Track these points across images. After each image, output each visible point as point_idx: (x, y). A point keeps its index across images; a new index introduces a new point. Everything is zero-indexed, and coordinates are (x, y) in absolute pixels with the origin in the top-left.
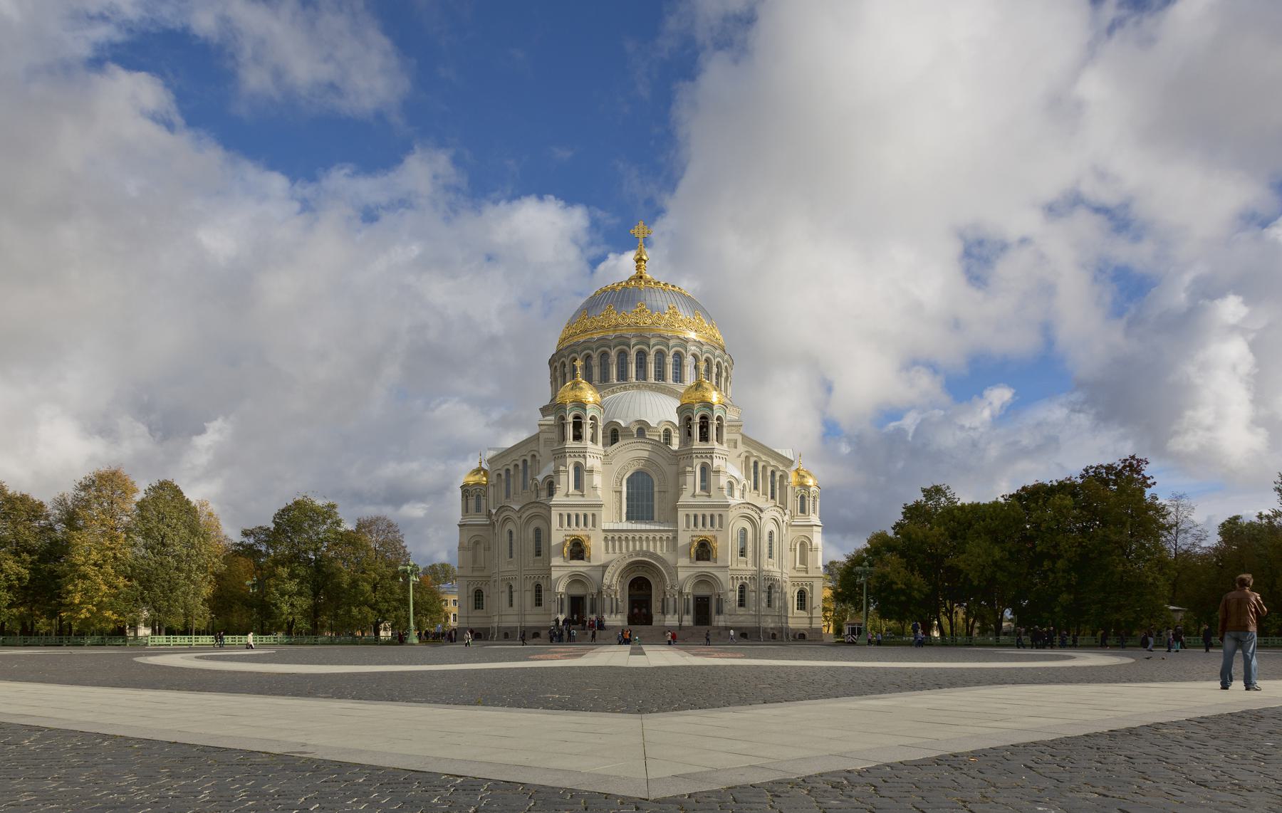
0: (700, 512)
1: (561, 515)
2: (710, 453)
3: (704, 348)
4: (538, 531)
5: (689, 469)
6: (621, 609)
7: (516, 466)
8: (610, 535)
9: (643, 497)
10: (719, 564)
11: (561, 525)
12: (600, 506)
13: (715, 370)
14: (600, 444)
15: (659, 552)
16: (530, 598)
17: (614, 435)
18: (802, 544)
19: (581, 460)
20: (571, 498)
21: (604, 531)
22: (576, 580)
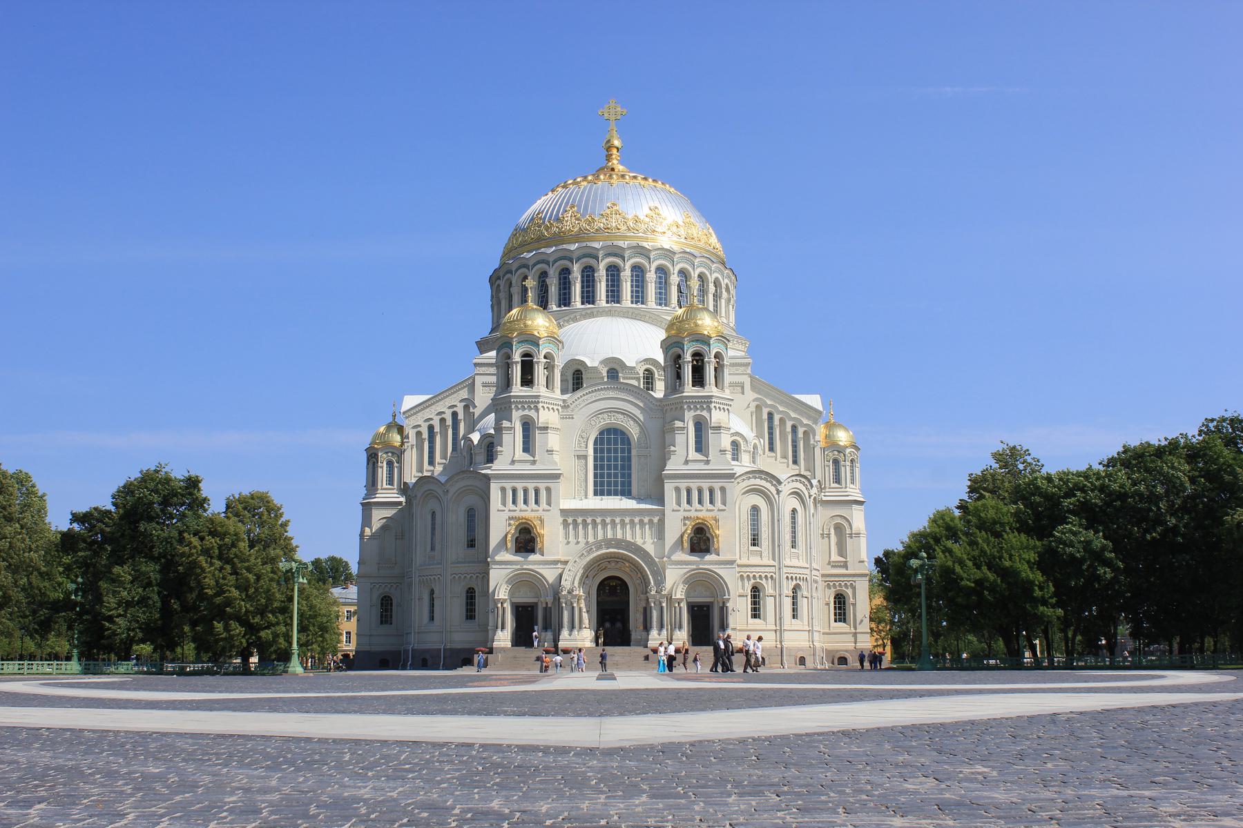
0: (694, 484)
1: (503, 490)
2: (706, 402)
3: (697, 261)
4: (471, 514)
5: (678, 424)
7: (443, 421)
9: (616, 462)
10: (721, 558)
11: (504, 504)
12: (557, 477)
13: (712, 288)
14: (558, 391)
15: (639, 542)
16: (456, 608)
17: (576, 378)
18: (839, 529)
19: (532, 413)
20: (517, 466)
21: (564, 512)
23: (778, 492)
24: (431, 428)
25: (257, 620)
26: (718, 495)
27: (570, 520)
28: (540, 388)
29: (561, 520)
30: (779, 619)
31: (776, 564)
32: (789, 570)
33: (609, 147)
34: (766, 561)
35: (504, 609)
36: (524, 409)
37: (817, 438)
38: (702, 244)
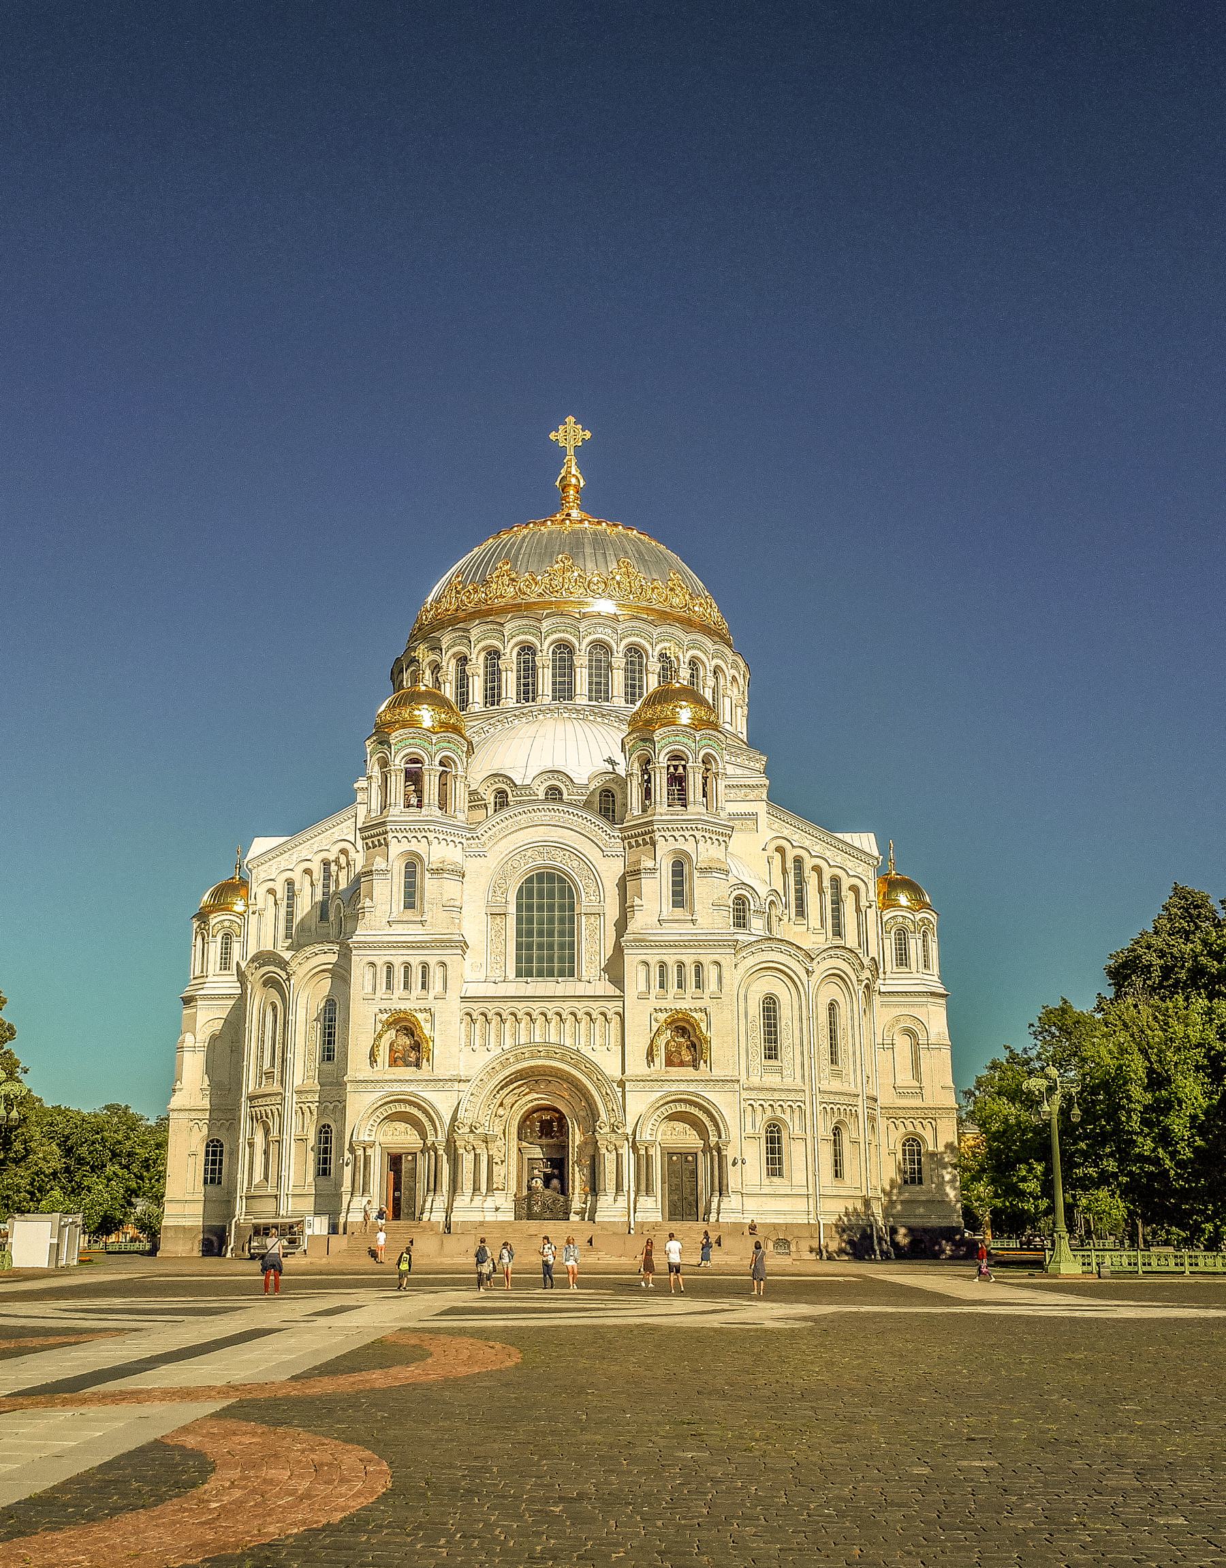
6: (498, 1181)
8: (477, 1008)
10: (717, 1073)
15: (586, 1051)
19: (421, 848)
23: (807, 971)
24: (290, 883)
28: (431, 810)
31: (807, 1088)
34: (788, 1082)
35: (367, 1159)
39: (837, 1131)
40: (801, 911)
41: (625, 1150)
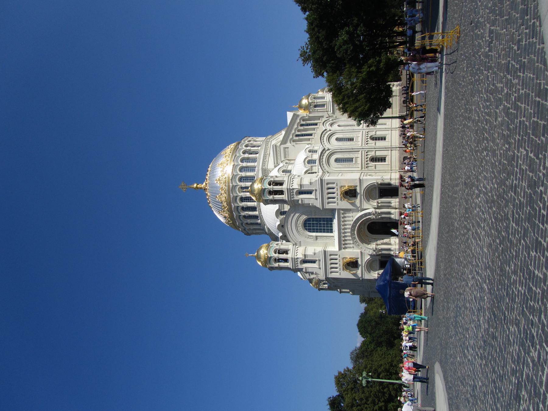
0: (326, 196)
2: (290, 191)
5: (300, 202)
10: (358, 184)
12: (325, 252)
19: (299, 260)
20: (321, 267)
22: (370, 266)
23: (329, 150)
25: (387, 395)
26: (330, 186)
27: (344, 246)
28: (289, 256)
29: (343, 250)
30: (386, 149)
32: (364, 143)
33: (197, 188)
34: (360, 155)
36: (297, 263)
37: (305, 115)
38: (229, 159)
39: (373, 138)
40: (311, 135)
41: (379, 211)
